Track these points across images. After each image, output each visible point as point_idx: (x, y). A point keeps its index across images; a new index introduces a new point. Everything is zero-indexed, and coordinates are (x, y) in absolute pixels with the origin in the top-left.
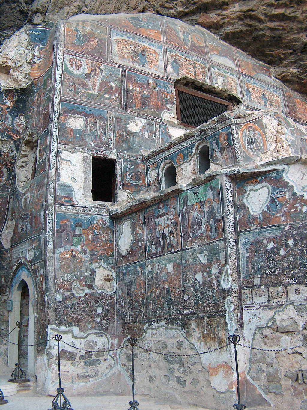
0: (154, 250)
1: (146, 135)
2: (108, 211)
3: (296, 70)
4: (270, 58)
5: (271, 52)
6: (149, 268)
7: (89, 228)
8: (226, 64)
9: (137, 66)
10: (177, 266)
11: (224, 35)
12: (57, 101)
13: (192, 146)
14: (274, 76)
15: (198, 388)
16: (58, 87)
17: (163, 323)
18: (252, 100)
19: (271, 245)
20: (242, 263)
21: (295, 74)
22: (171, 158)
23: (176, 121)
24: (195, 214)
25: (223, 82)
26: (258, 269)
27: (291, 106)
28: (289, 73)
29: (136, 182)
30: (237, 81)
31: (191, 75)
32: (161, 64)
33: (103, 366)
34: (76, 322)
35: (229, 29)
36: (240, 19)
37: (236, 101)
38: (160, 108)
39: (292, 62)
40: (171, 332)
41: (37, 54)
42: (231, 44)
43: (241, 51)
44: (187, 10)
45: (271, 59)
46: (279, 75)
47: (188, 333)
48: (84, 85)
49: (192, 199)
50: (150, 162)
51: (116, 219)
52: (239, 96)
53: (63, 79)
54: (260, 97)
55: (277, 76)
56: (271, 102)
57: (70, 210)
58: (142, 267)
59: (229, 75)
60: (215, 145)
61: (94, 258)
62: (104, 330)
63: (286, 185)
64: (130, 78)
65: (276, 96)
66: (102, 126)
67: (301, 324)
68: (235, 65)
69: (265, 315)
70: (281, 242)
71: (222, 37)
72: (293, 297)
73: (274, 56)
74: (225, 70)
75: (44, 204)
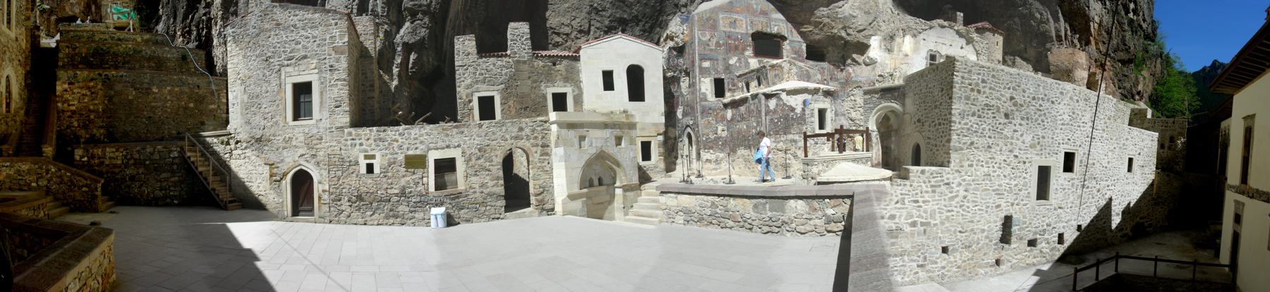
1: (738, 65)
7: (714, 110)
9: (732, 30)
12: (697, 55)
16: (697, 48)
29: (734, 88)
31: (760, 28)
33: (723, 164)
34: (711, 148)
38: (744, 49)
41: (685, 28)
48: (708, 45)
51: (726, 106)
53: (699, 45)
57: (706, 103)
61: (717, 122)
62: (722, 151)
64: (729, 37)
66: (717, 64)
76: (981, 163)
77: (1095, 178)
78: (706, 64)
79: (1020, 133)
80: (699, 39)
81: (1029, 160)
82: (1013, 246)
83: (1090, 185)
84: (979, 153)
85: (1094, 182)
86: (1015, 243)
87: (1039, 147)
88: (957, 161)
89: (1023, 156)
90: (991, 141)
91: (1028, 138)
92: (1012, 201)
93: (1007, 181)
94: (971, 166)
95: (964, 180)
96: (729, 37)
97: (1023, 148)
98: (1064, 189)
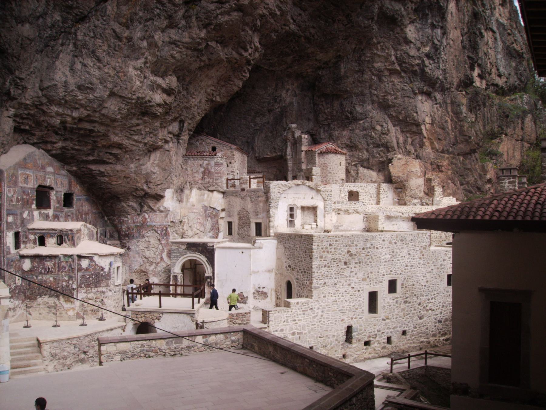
0: (43, 271)
2: (20, 254)
6: (40, 278)
9: (26, 186)
10: (55, 279)
13: (55, 234)
15: (62, 315)
16: (5, 204)
17: (47, 296)
19: (88, 277)
20: (79, 280)
22: (44, 234)
23: (35, 208)
24: (64, 264)
26: (83, 283)
29: (26, 240)
32: (32, 181)
35: (54, 152)
36: (60, 148)
37: (52, 189)
38: (32, 203)
40: (51, 299)
44: (39, 142)
47: (59, 299)
48: (12, 201)
49: (62, 259)
50: (30, 231)
51: (23, 257)
52: (54, 187)
58: (37, 277)
59: (51, 177)
60: (66, 238)
63: (94, 261)
67: (95, 297)
69: (85, 295)
70: (91, 276)
72: (93, 290)
75: (2, 255)
76: (331, 295)
77: (415, 295)
78: (10, 219)
79: (354, 273)
80: (7, 196)
81: (362, 289)
82: (354, 345)
83: (412, 301)
84: (329, 289)
85: (415, 298)
86: (355, 343)
87: (368, 280)
88: (317, 295)
89: (357, 287)
90: (336, 280)
91: (361, 275)
92: (352, 316)
93: (348, 304)
94: (325, 297)
95: (321, 306)
96: (24, 192)
97: (357, 282)
98: (390, 306)
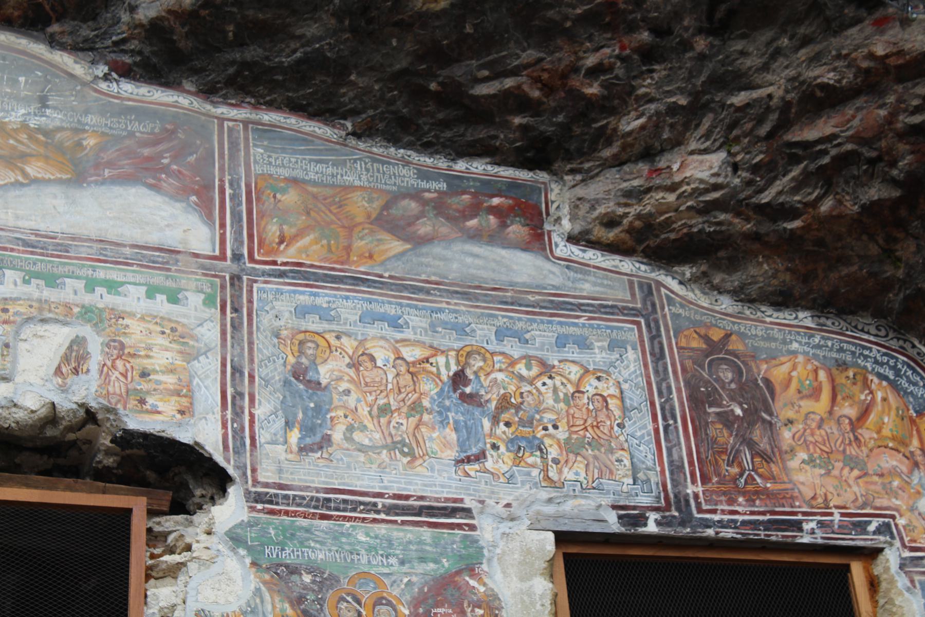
3: (717, 159)
4: (517, 120)
5: (509, 83)
8: (132, 234)
11: (133, 45)
14: (572, 239)
18: (337, 435)
21: (716, 187)
25: (66, 358)
27: (727, 419)
28: (672, 188)
30: (210, 333)
39: (673, 109)
42: (208, 92)
43: (293, 121)
45: (524, 128)
46: (610, 222)
54: (416, 408)
55: (599, 232)
56: (530, 422)
65: (574, 372)
68: (208, 216)
71: (127, 59)
73: (539, 103)
74: (101, 274)
